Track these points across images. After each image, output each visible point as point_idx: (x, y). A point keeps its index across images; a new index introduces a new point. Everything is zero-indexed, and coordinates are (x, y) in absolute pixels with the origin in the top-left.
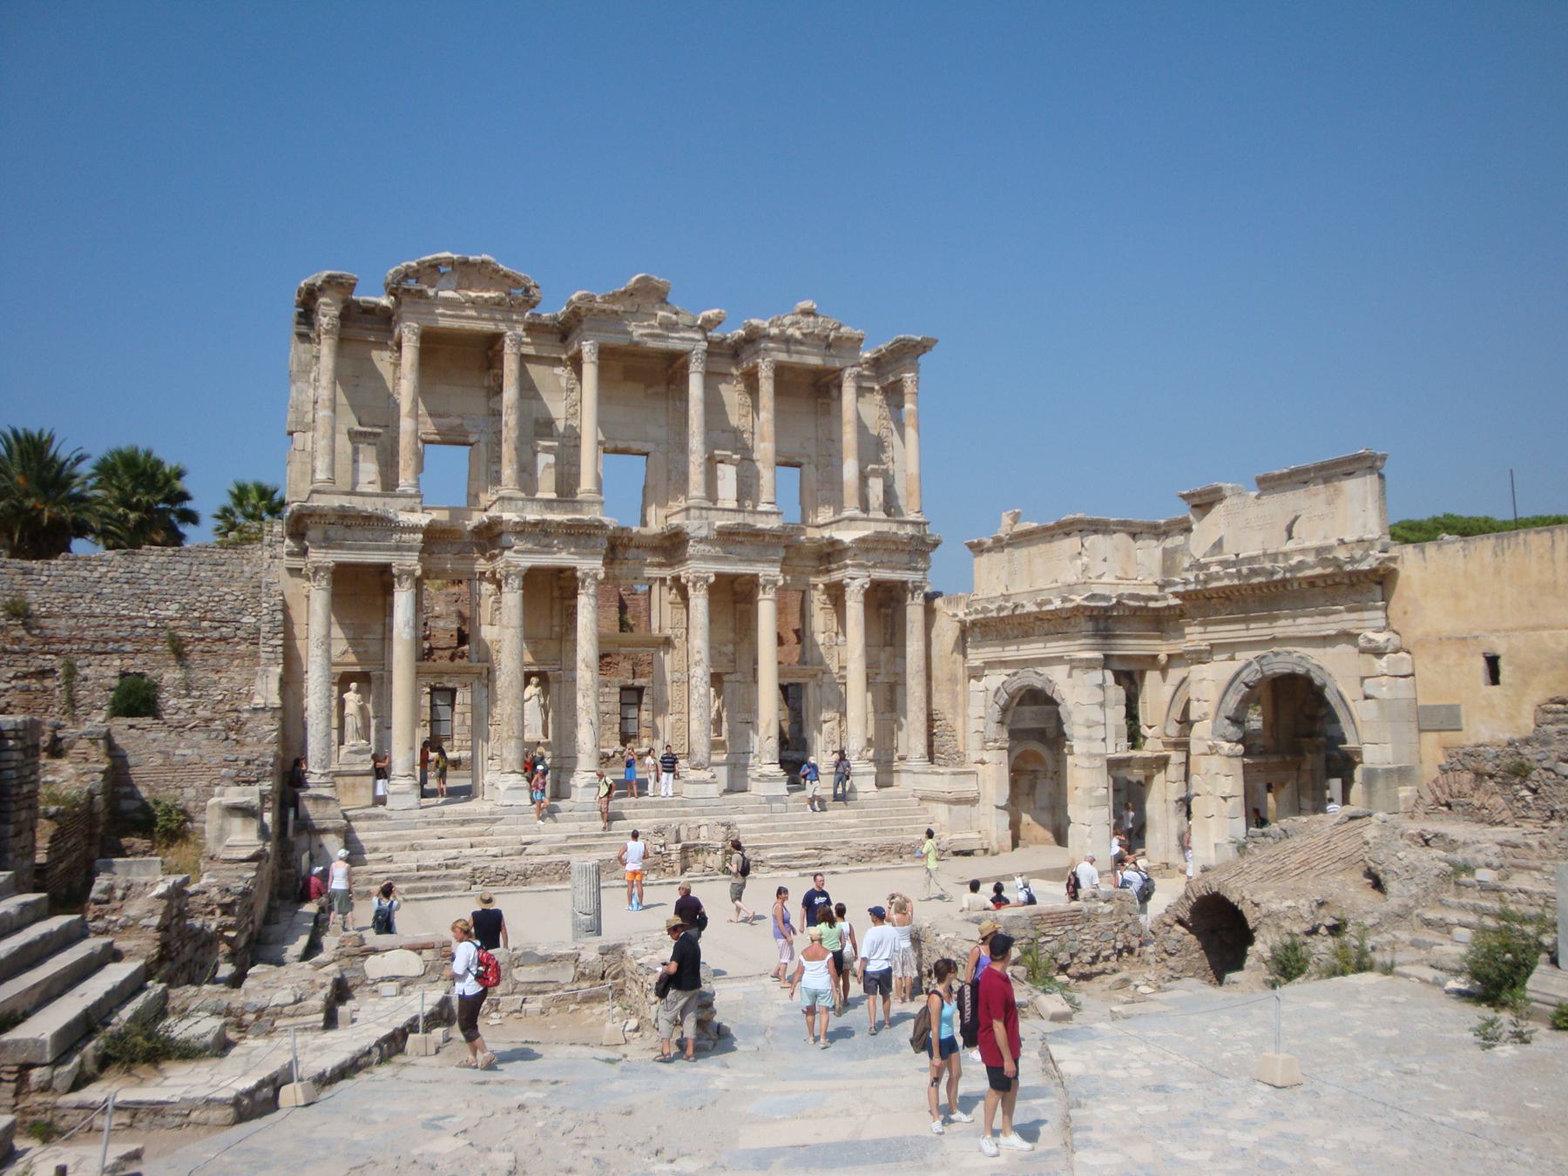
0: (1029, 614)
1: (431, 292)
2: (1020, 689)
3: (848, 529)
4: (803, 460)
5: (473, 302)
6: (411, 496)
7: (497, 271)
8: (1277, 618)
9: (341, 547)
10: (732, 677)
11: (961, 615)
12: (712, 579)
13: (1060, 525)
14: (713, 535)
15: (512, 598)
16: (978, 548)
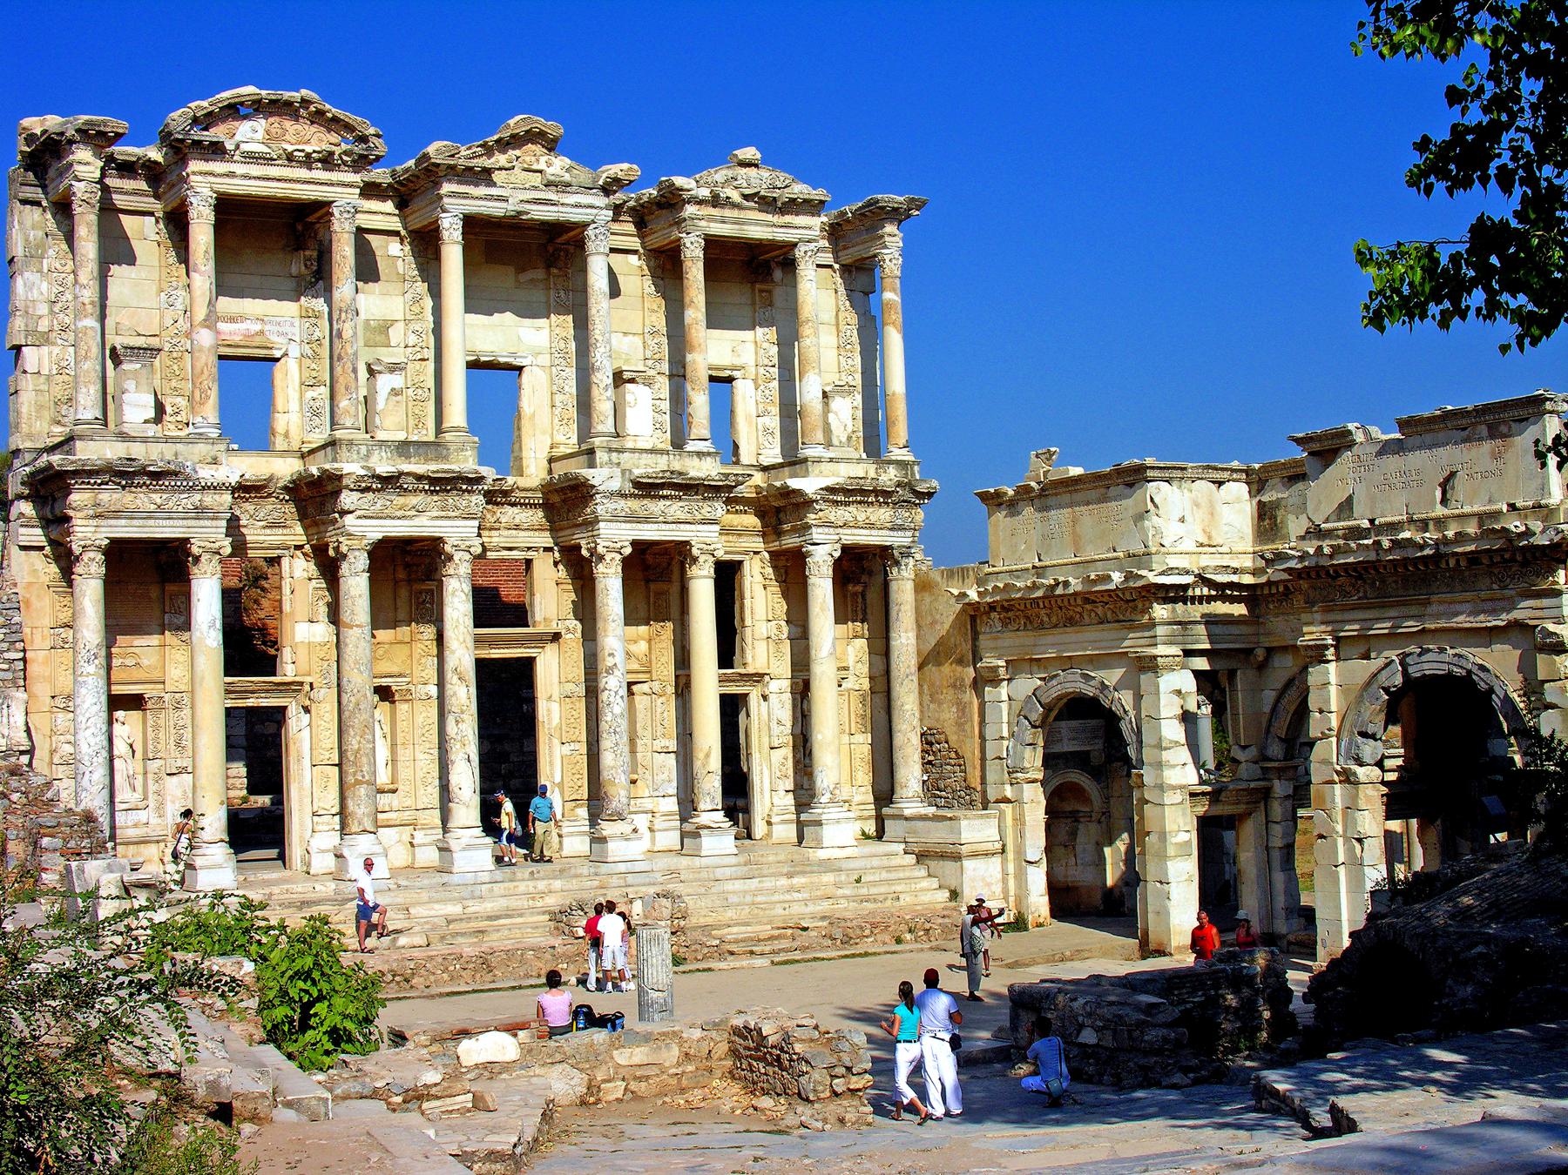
0: (1076, 594)
1: (229, 146)
2: (1059, 698)
3: (806, 474)
4: (736, 374)
5: (290, 158)
6: (214, 442)
7: (320, 113)
8: (1427, 603)
9: (116, 514)
10: (645, 687)
11: (973, 595)
12: (628, 551)
13: (1119, 472)
14: (628, 488)
15: (356, 583)
16: (993, 500)
